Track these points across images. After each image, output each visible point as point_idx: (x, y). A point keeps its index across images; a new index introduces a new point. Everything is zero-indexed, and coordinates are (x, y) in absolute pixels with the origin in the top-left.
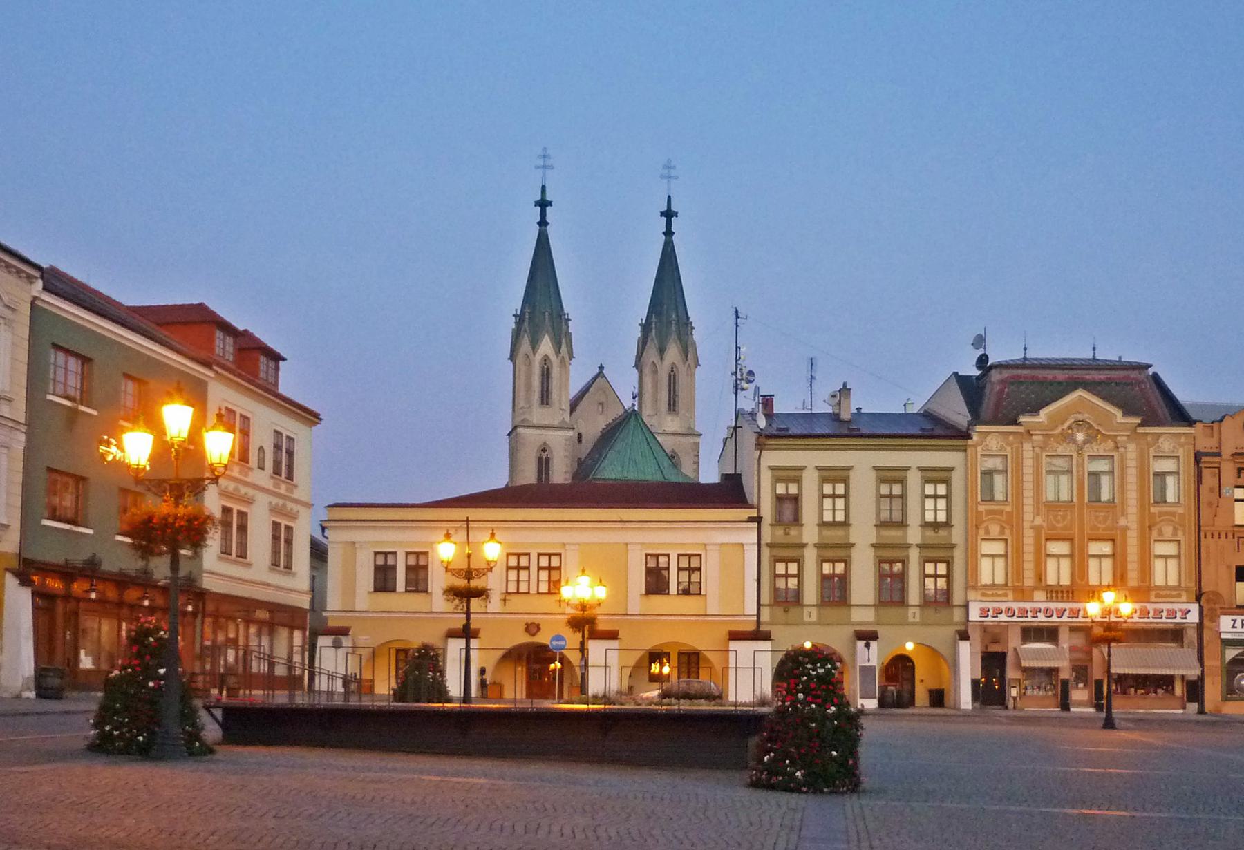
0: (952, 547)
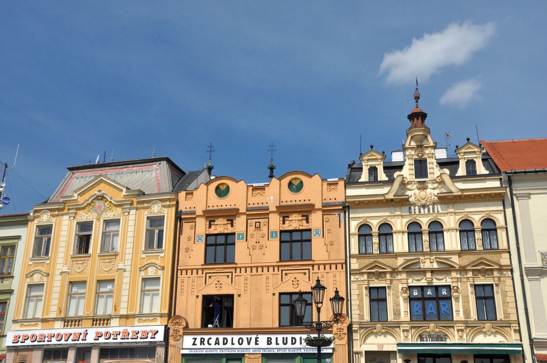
0: (11, 292)
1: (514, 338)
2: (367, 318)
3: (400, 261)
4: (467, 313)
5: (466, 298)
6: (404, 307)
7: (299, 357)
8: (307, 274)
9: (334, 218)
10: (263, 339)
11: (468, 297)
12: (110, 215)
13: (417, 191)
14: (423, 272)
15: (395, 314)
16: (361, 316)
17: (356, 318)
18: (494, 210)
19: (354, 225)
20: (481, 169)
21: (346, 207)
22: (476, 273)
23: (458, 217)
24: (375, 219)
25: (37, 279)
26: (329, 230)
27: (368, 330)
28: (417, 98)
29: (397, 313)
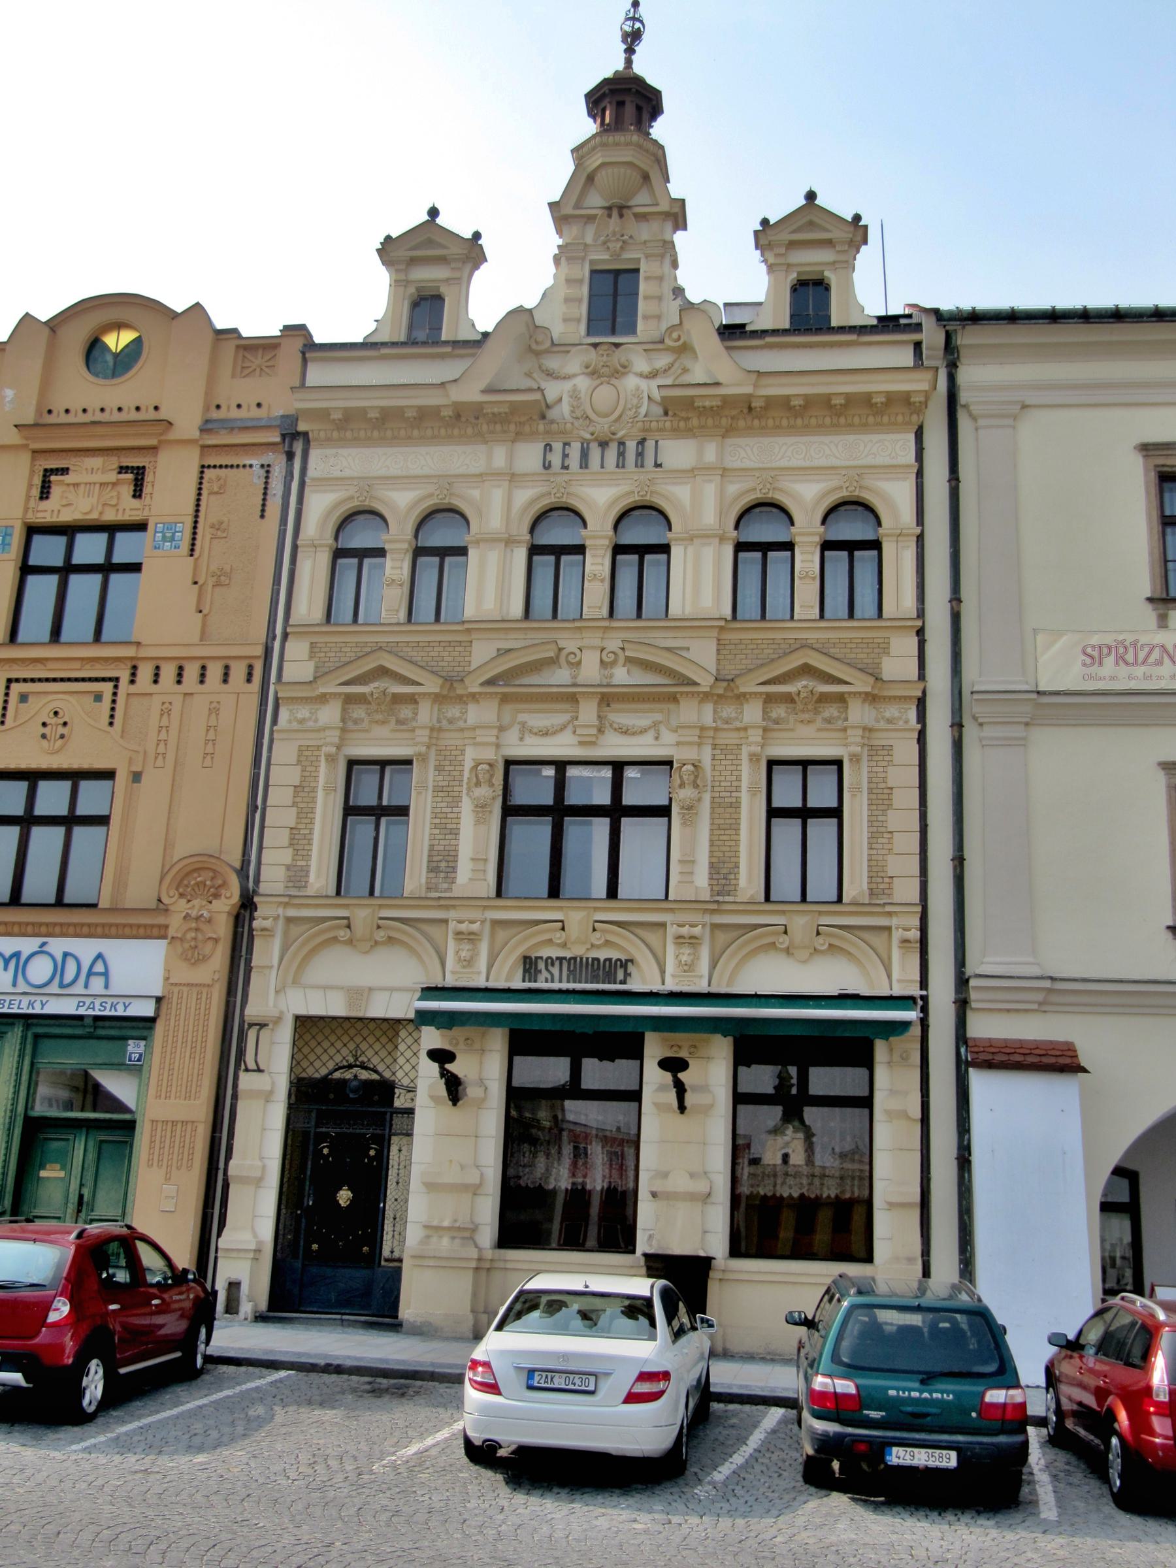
1: (904, 981)
2: (321, 877)
5: (725, 810)
6: (476, 838)
7: (18, 1030)
8: (107, 697)
11: (736, 806)
13: (583, 383)
15: (433, 869)
16: (297, 875)
17: (273, 878)
18: (880, 463)
19: (320, 509)
22: (779, 711)
23: (733, 489)
26: (217, 527)
28: (632, 38)
29: (443, 864)
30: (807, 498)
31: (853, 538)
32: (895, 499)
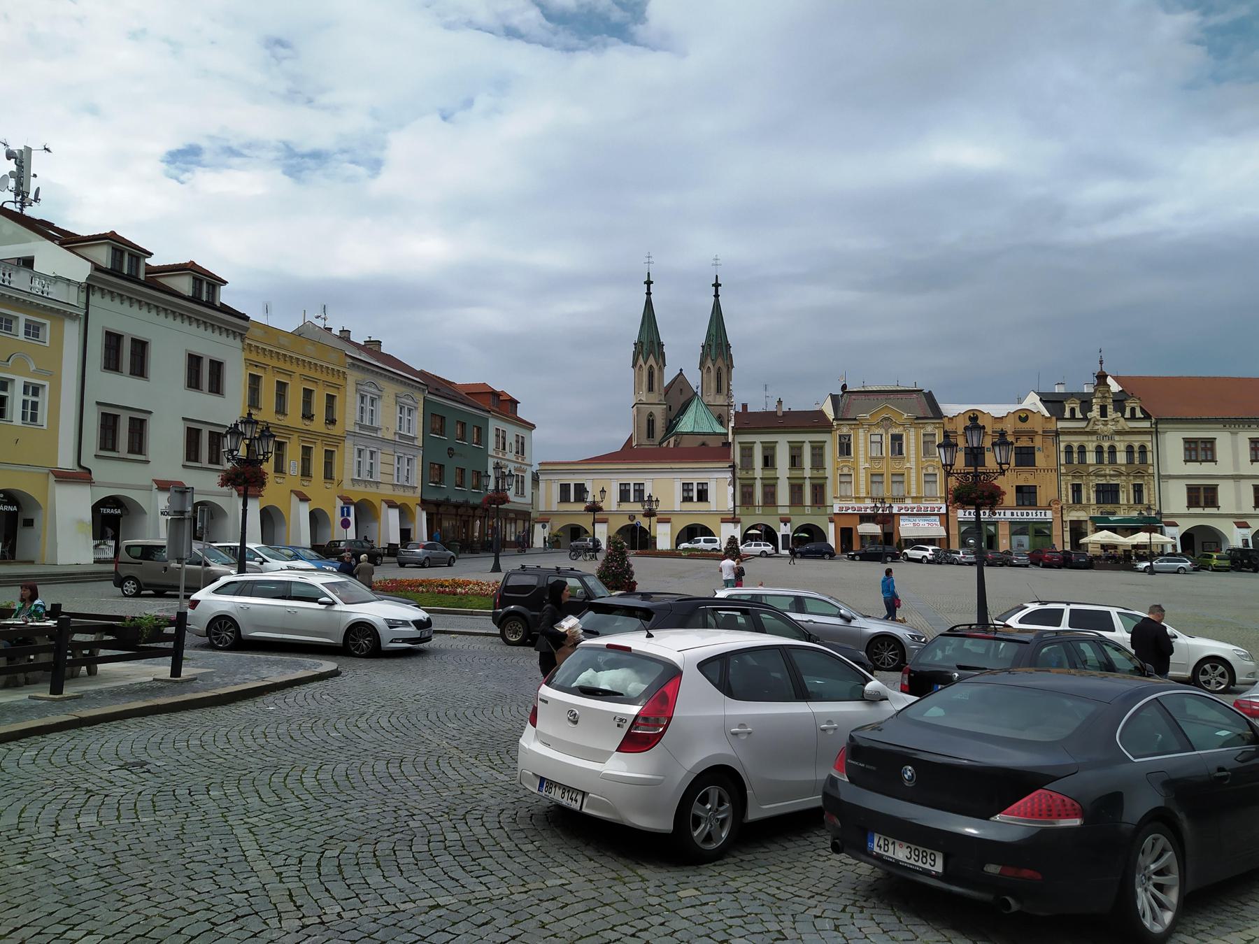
3: (1091, 469)
4: (1128, 500)
6: (1093, 496)
9: (1049, 441)
10: (1008, 513)
12: (896, 431)
14: (1105, 476)
19: (1062, 445)
20: (1139, 414)
21: (1057, 433)
24: (1075, 441)
25: (846, 471)
27: (1070, 508)
28: (1101, 363)
29: (1088, 499)
30: (1136, 445)
31: (1143, 450)
32: (1149, 445)
